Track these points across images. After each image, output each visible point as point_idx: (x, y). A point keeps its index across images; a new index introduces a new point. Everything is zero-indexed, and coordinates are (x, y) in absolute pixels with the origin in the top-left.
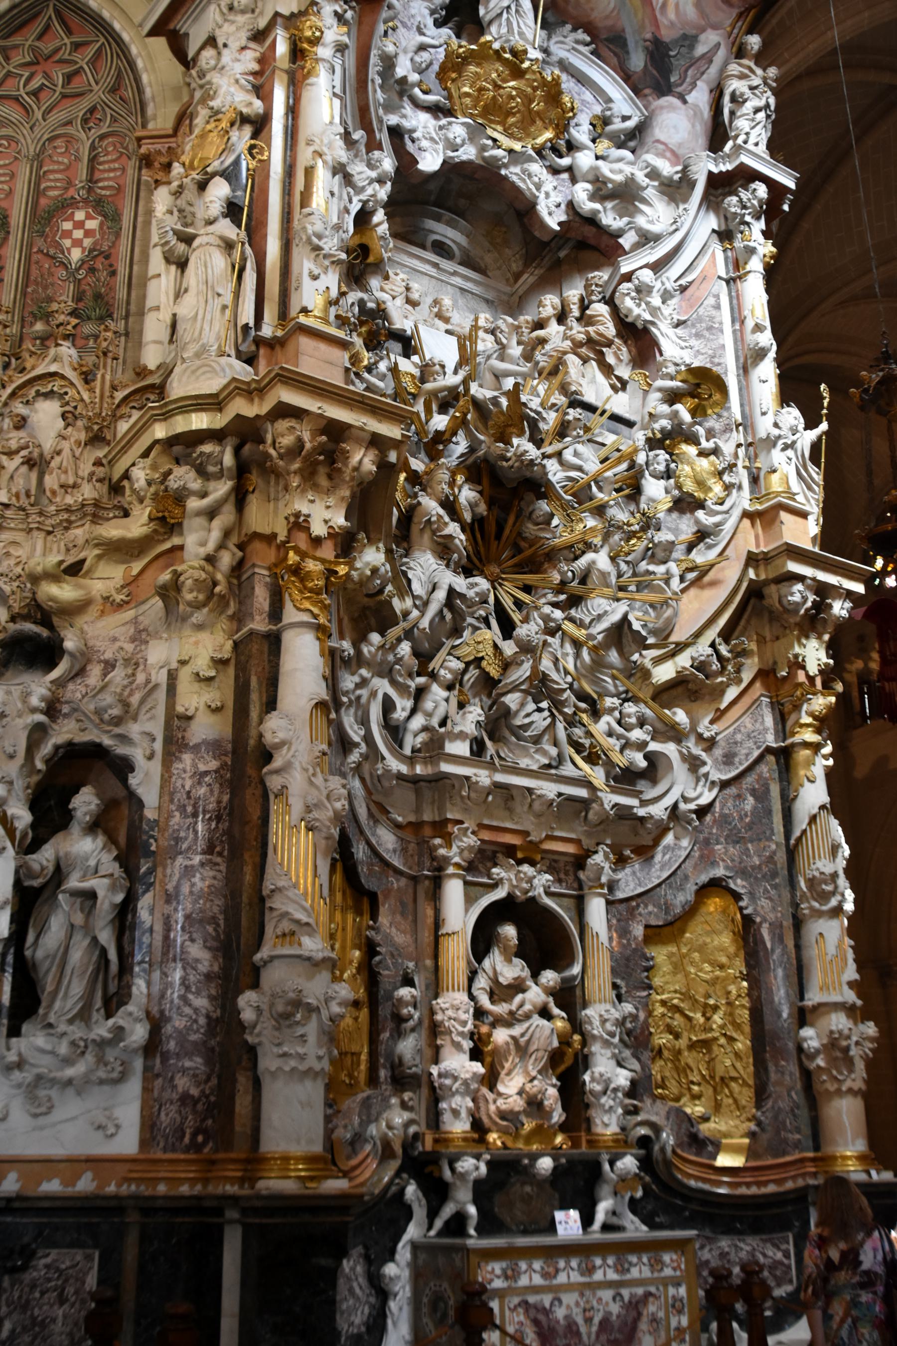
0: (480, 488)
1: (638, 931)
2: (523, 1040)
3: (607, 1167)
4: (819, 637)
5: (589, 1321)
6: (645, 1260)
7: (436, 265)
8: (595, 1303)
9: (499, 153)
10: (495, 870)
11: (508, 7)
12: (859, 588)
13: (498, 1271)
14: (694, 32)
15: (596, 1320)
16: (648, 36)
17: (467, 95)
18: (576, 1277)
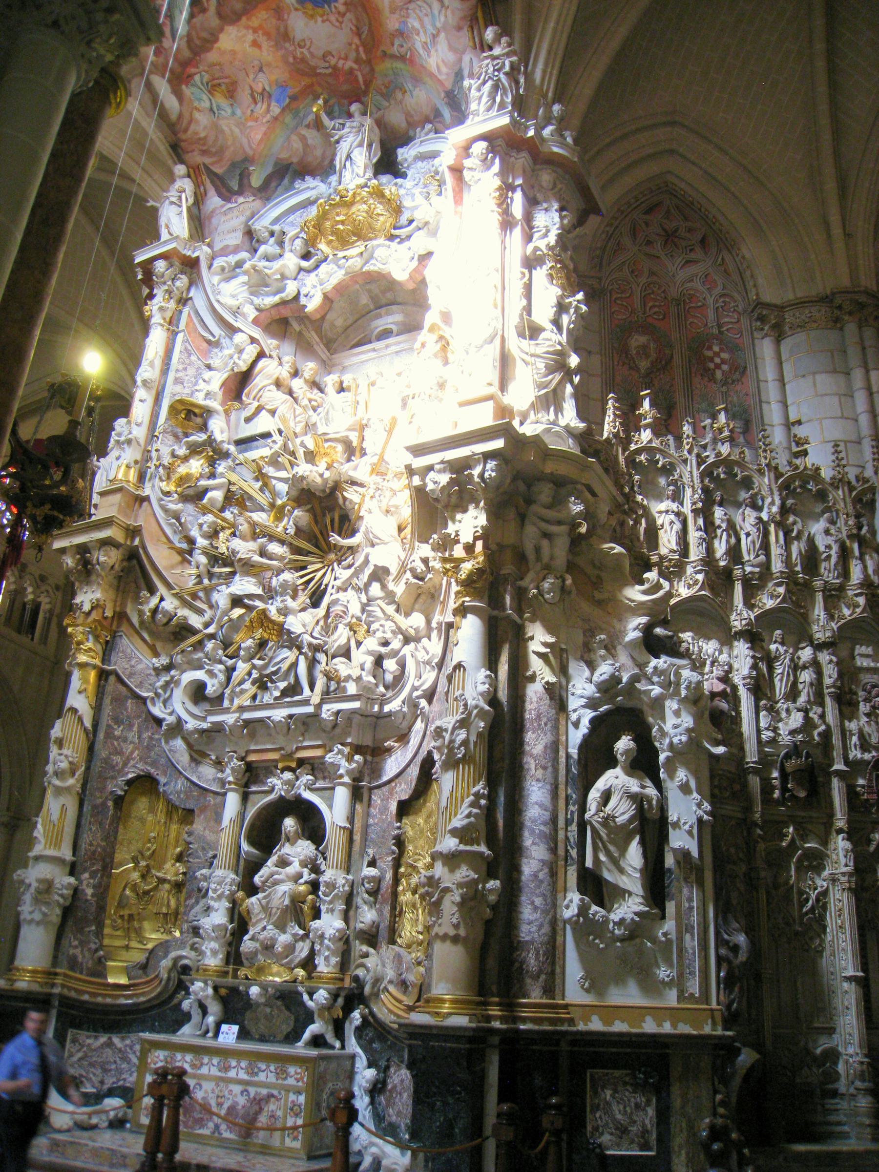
0: (309, 506)
1: (393, 807)
2: (264, 902)
3: (306, 997)
4: (477, 507)
5: (220, 1105)
6: (272, 1068)
7: (374, 350)
8: (226, 1093)
9: (350, 261)
10: (269, 780)
11: (345, 167)
12: (498, 444)
13: (162, 1058)
14: (456, 69)
15: (226, 1106)
16: (443, 95)
17: (332, 241)
18: (214, 1071)
